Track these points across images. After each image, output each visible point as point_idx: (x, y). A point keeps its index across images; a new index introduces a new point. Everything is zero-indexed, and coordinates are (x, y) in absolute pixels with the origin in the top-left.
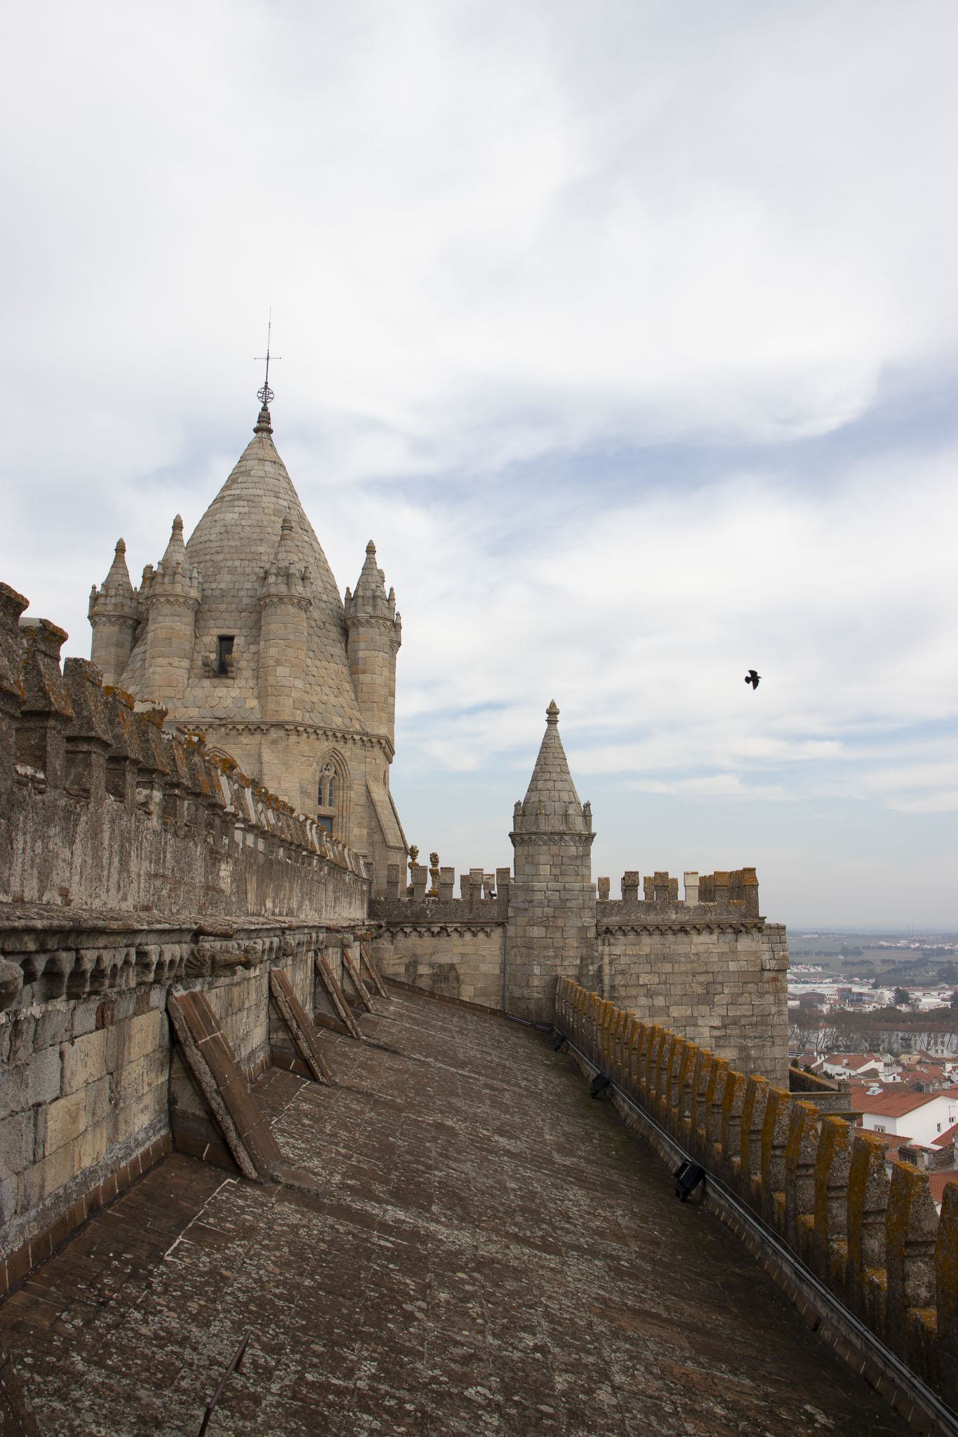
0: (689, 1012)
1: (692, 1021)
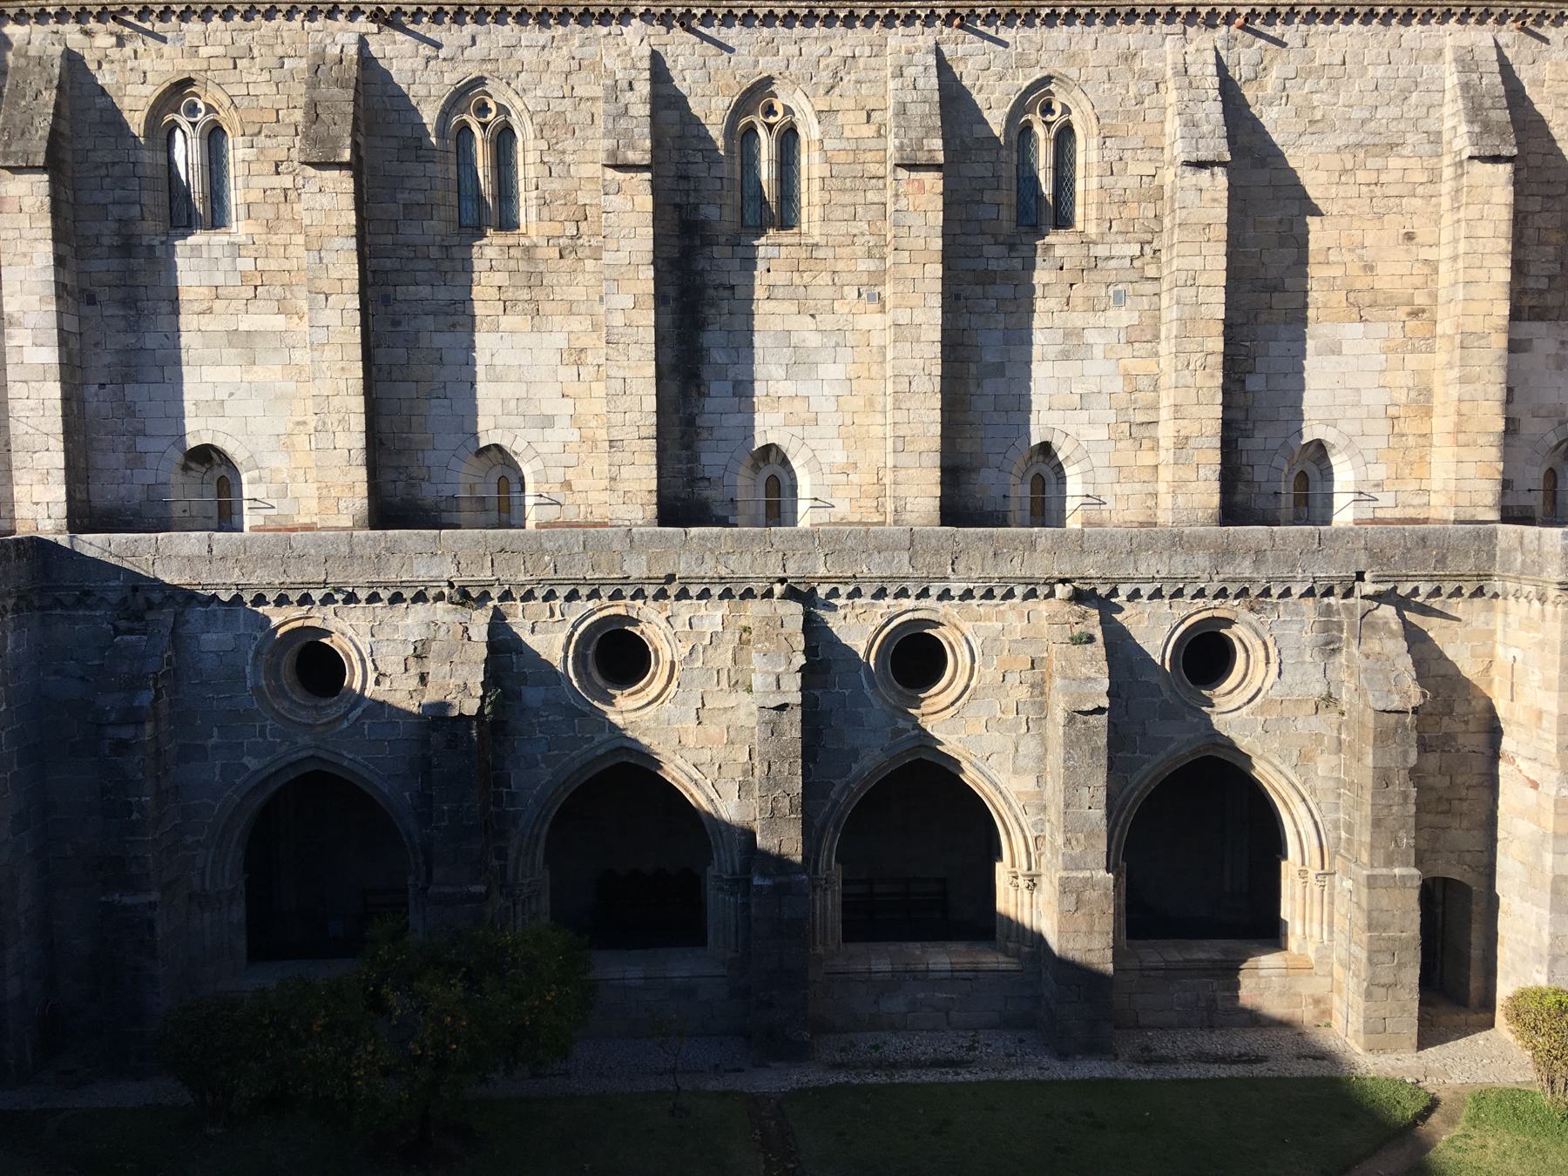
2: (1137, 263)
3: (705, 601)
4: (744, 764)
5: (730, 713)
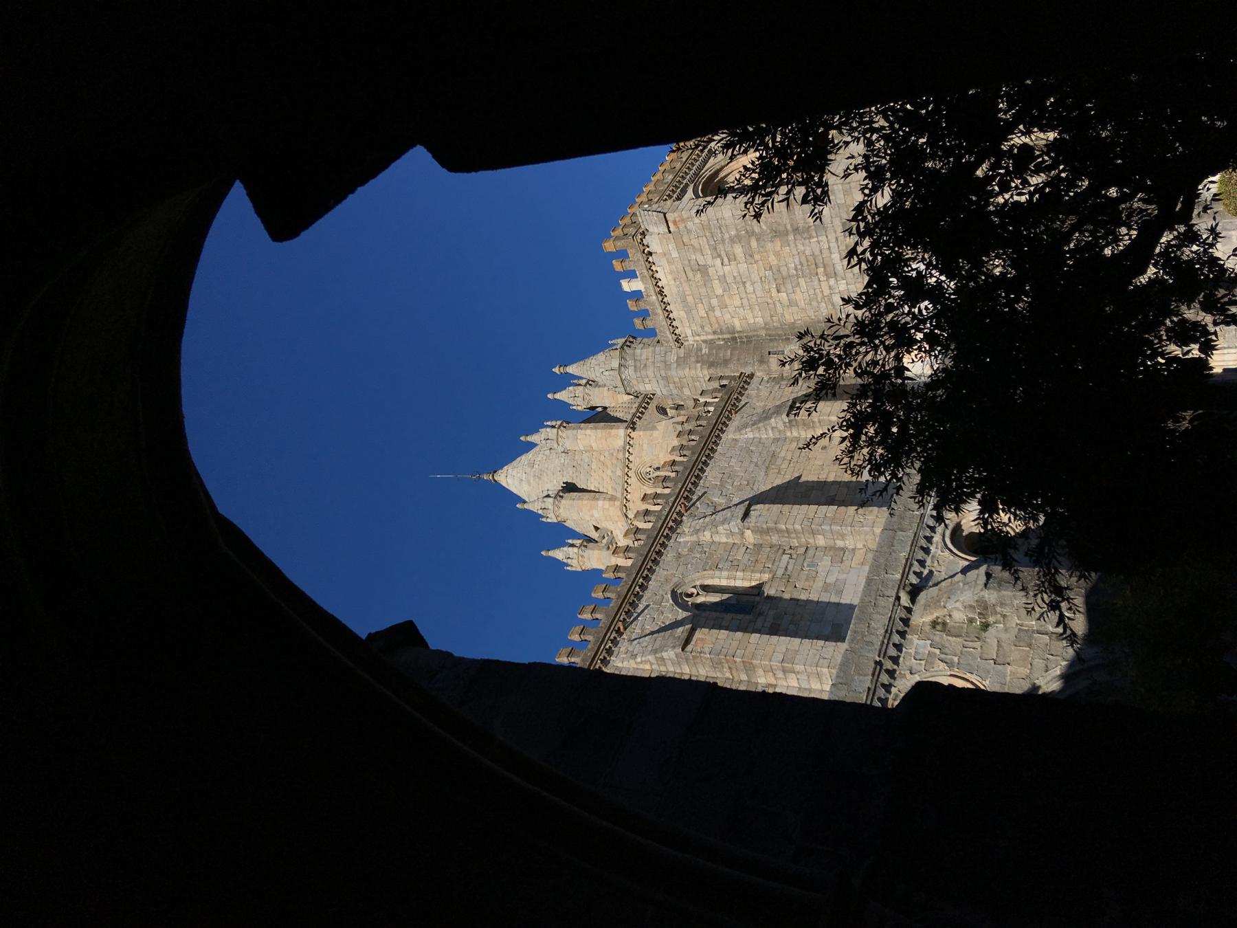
0: (717, 282)
1: (723, 279)
2: (794, 556)
3: (904, 649)
4: (1050, 639)
5: (1003, 644)
